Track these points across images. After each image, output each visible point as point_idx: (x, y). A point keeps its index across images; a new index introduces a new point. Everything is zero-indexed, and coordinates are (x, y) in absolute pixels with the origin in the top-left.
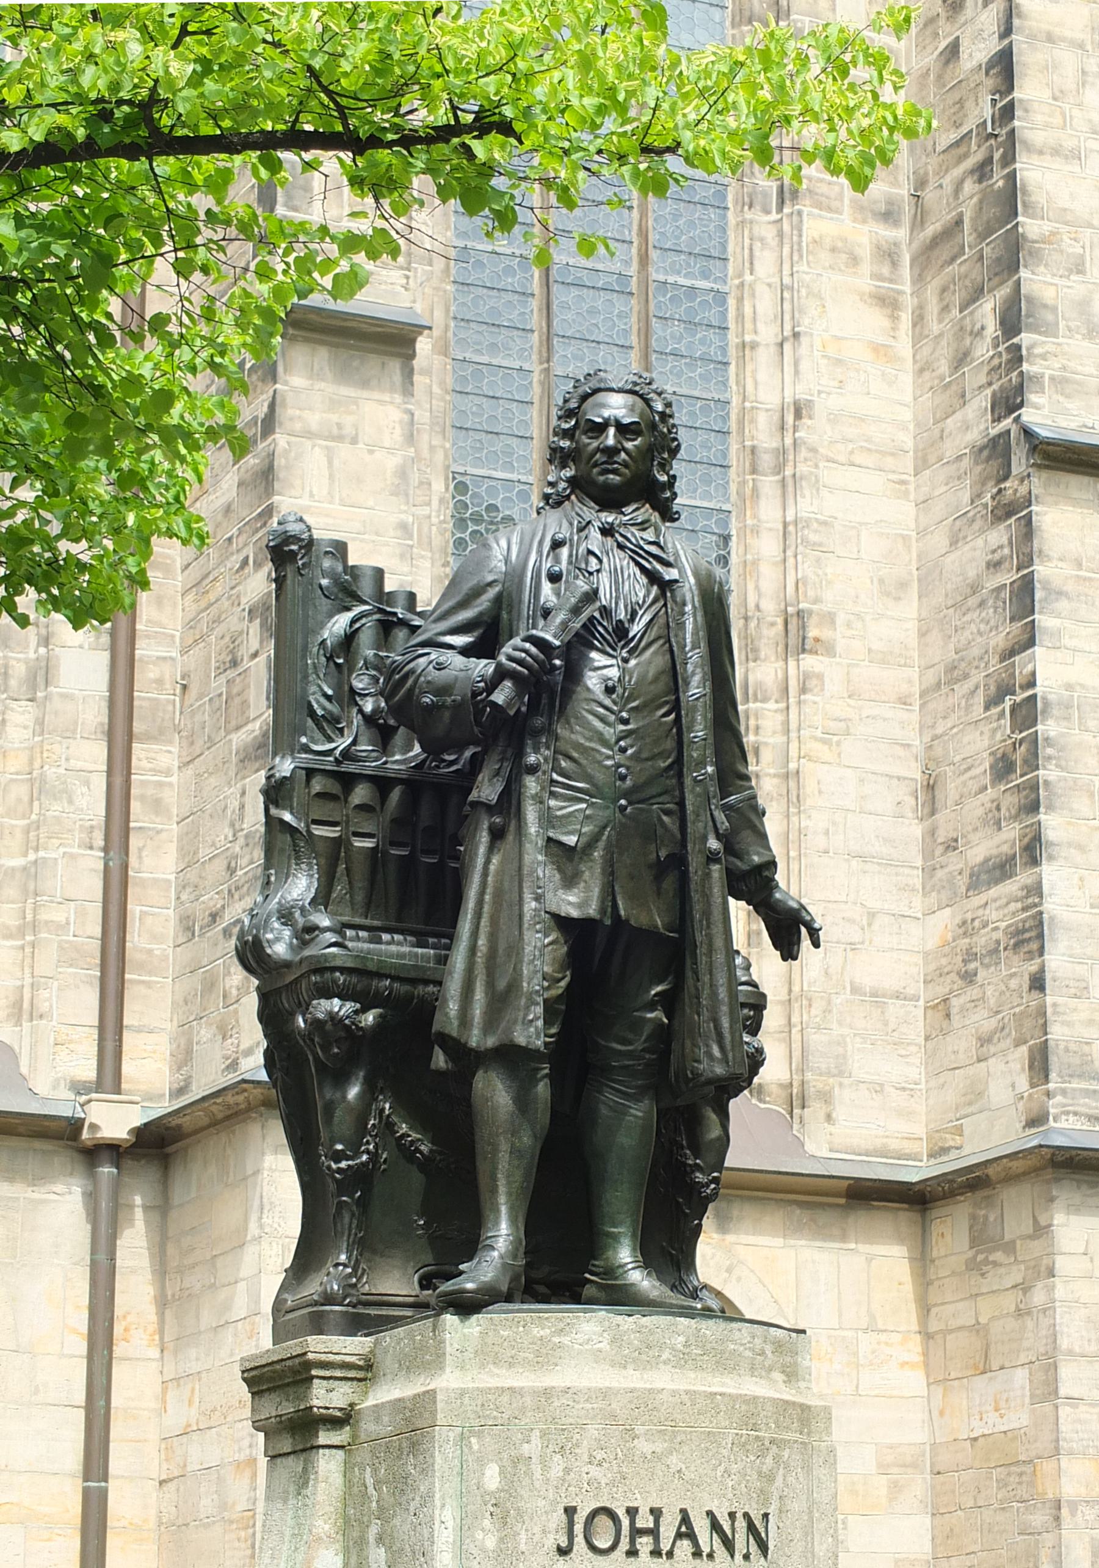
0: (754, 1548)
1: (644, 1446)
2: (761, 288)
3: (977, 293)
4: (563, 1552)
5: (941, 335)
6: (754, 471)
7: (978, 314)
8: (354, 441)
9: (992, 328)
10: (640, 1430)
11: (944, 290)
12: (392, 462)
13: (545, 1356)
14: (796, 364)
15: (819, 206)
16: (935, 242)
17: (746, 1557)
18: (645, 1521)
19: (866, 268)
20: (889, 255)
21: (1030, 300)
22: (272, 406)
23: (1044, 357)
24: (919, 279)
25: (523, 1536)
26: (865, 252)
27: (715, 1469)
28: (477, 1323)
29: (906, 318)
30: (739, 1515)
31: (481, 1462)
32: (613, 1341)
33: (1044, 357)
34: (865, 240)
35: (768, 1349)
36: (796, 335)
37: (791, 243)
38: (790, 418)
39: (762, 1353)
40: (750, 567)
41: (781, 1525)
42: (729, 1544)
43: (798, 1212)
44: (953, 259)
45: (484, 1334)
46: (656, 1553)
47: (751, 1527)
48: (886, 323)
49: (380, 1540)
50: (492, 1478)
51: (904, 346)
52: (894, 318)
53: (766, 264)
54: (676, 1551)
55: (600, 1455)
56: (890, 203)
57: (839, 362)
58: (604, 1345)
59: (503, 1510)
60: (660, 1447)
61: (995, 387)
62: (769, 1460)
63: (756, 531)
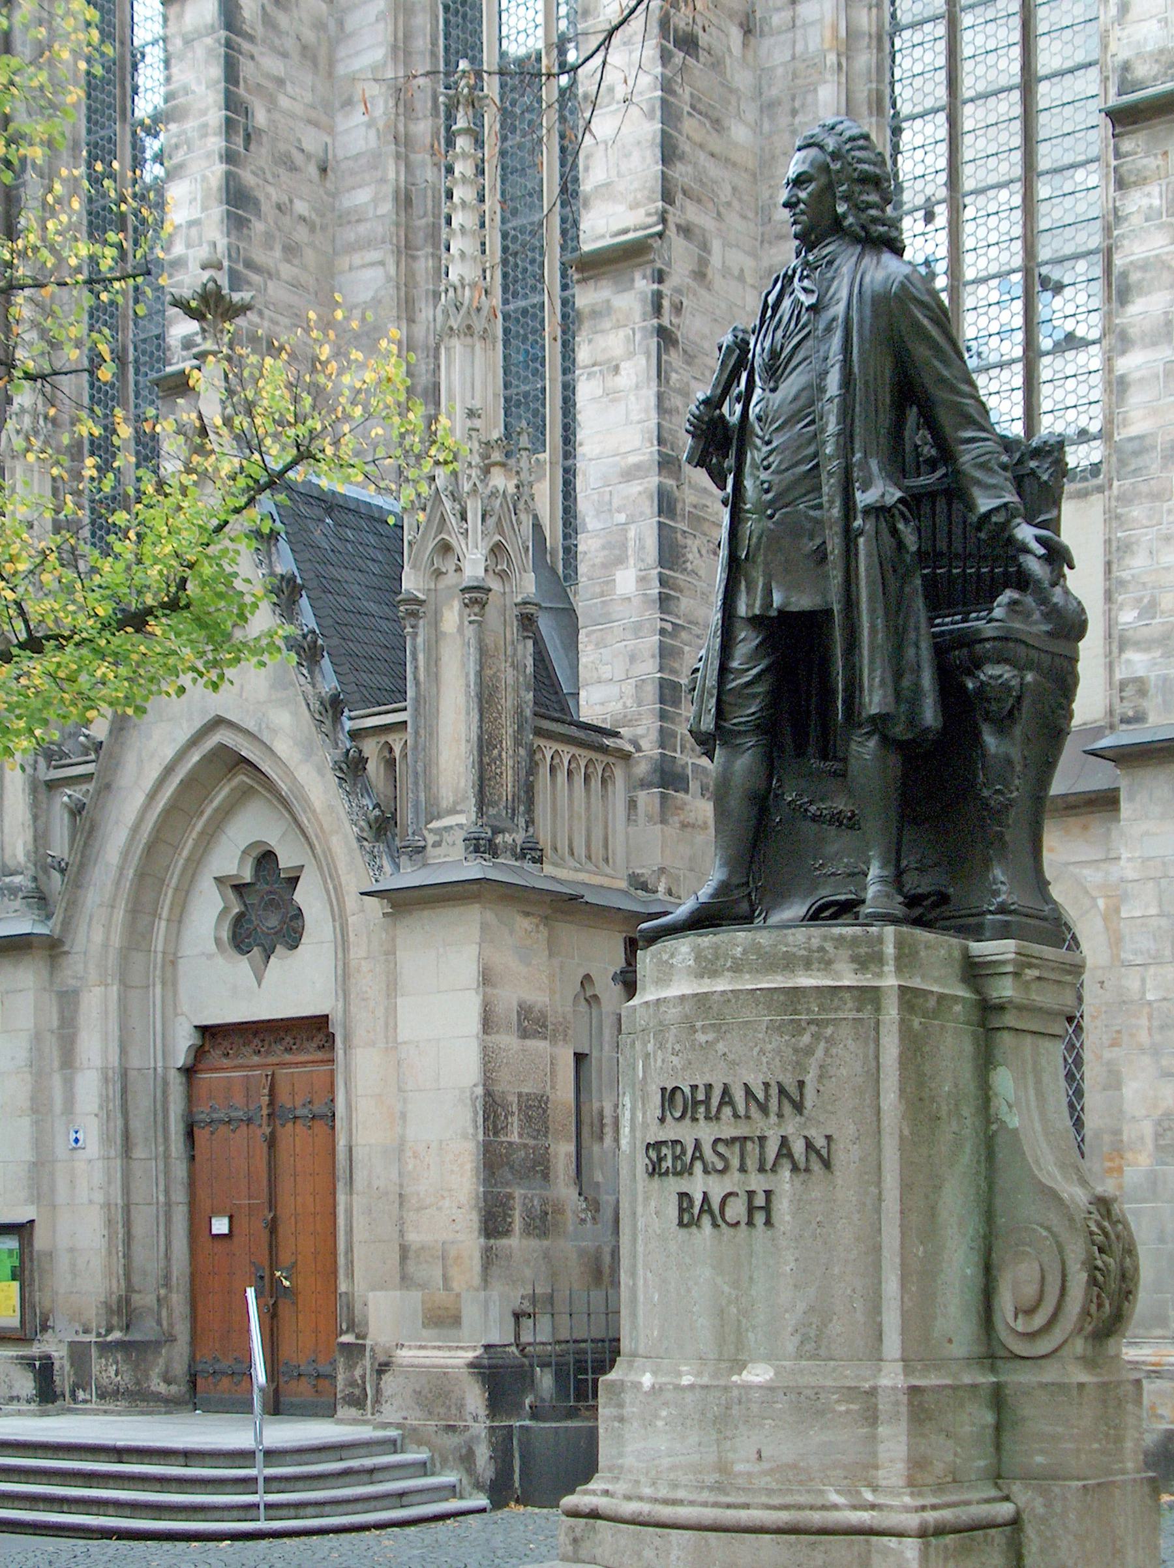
0: (788, 1109)
1: (702, 1038)
4: (662, 1120)
10: (699, 1024)
17: (780, 1115)
18: (701, 1096)
27: (751, 1049)
30: (773, 1083)
35: (829, 946)
39: (821, 949)
41: (822, 1089)
42: (764, 1109)
46: (708, 1118)
47: (782, 1091)
54: (723, 1117)
55: (677, 1047)
58: (691, 962)
60: (710, 1036)
62: (806, 1039)
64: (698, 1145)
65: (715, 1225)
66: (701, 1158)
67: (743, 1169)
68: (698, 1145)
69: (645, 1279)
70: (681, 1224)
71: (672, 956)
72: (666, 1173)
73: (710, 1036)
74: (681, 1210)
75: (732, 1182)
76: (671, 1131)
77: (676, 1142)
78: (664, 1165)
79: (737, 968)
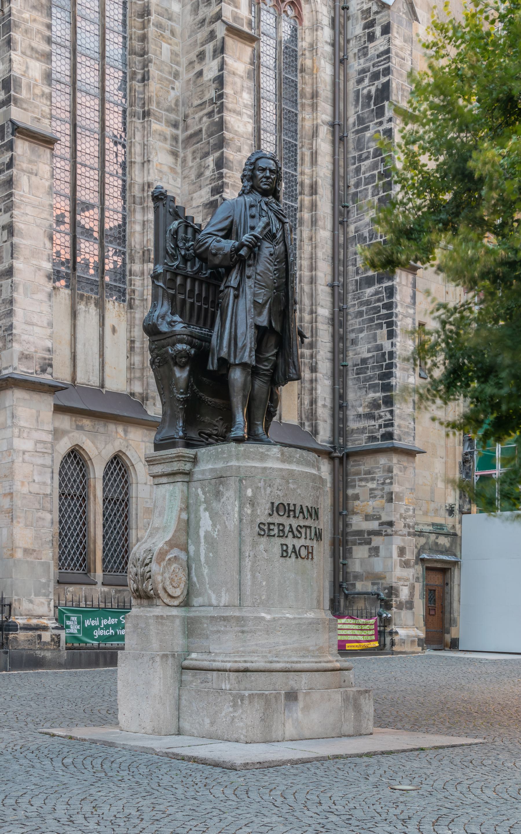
1: (291, 486)
2: (137, 144)
3: (206, 155)
4: (270, 515)
5: (191, 167)
6: (134, 203)
7: (207, 161)
8: (36, 175)
9: (212, 166)
10: (290, 481)
11: (194, 152)
12: (47, 184)
13: (263, 457)
14: (149, 170)
15: (156, 119)
16: (191, 136)
19: (169, 142)
20: (175, 138)
21: (226, 158)
22: (11, 159)
23: (229, 177)
24: (185, 148)
25: (259, 511)
26: (169, 137)
28: (242, 447)
29: (179, 160)
31: (246, 488)
32: (283, 454)
33: (229, 177)
34: (169, 133)
36: (149, 161)
37: (146, 131)
38: (146, 188)
40: (132, 233)
42: (311, 516)
43: (120, 429)
44: (198, 143)
45: (245, 450)
46: (295, 517)
48: (174, 161)
49: (206, 509)
50: (249, 492)
51: (179, 169)
52: (176, 160)
53: (138, 137)
56: (176, 122)
57: (160, 171)
59: (252, 502)
60: (295, 486)
61: (213, 185)
63: (134, 222)
64: (290, 525)
65: (297, 557)
66: (292, 531)
67: (306, 538)
68: (290, 525)
69: (254, 576)
70: (282, 556)
71: (268, 451)
72: (274, 536)
73: (295, 486)
74: (283, 551)
75: (302, 542)
76: (276, 519)
77: (279, 525)
78: (272, 533)
79: (298, 463)
